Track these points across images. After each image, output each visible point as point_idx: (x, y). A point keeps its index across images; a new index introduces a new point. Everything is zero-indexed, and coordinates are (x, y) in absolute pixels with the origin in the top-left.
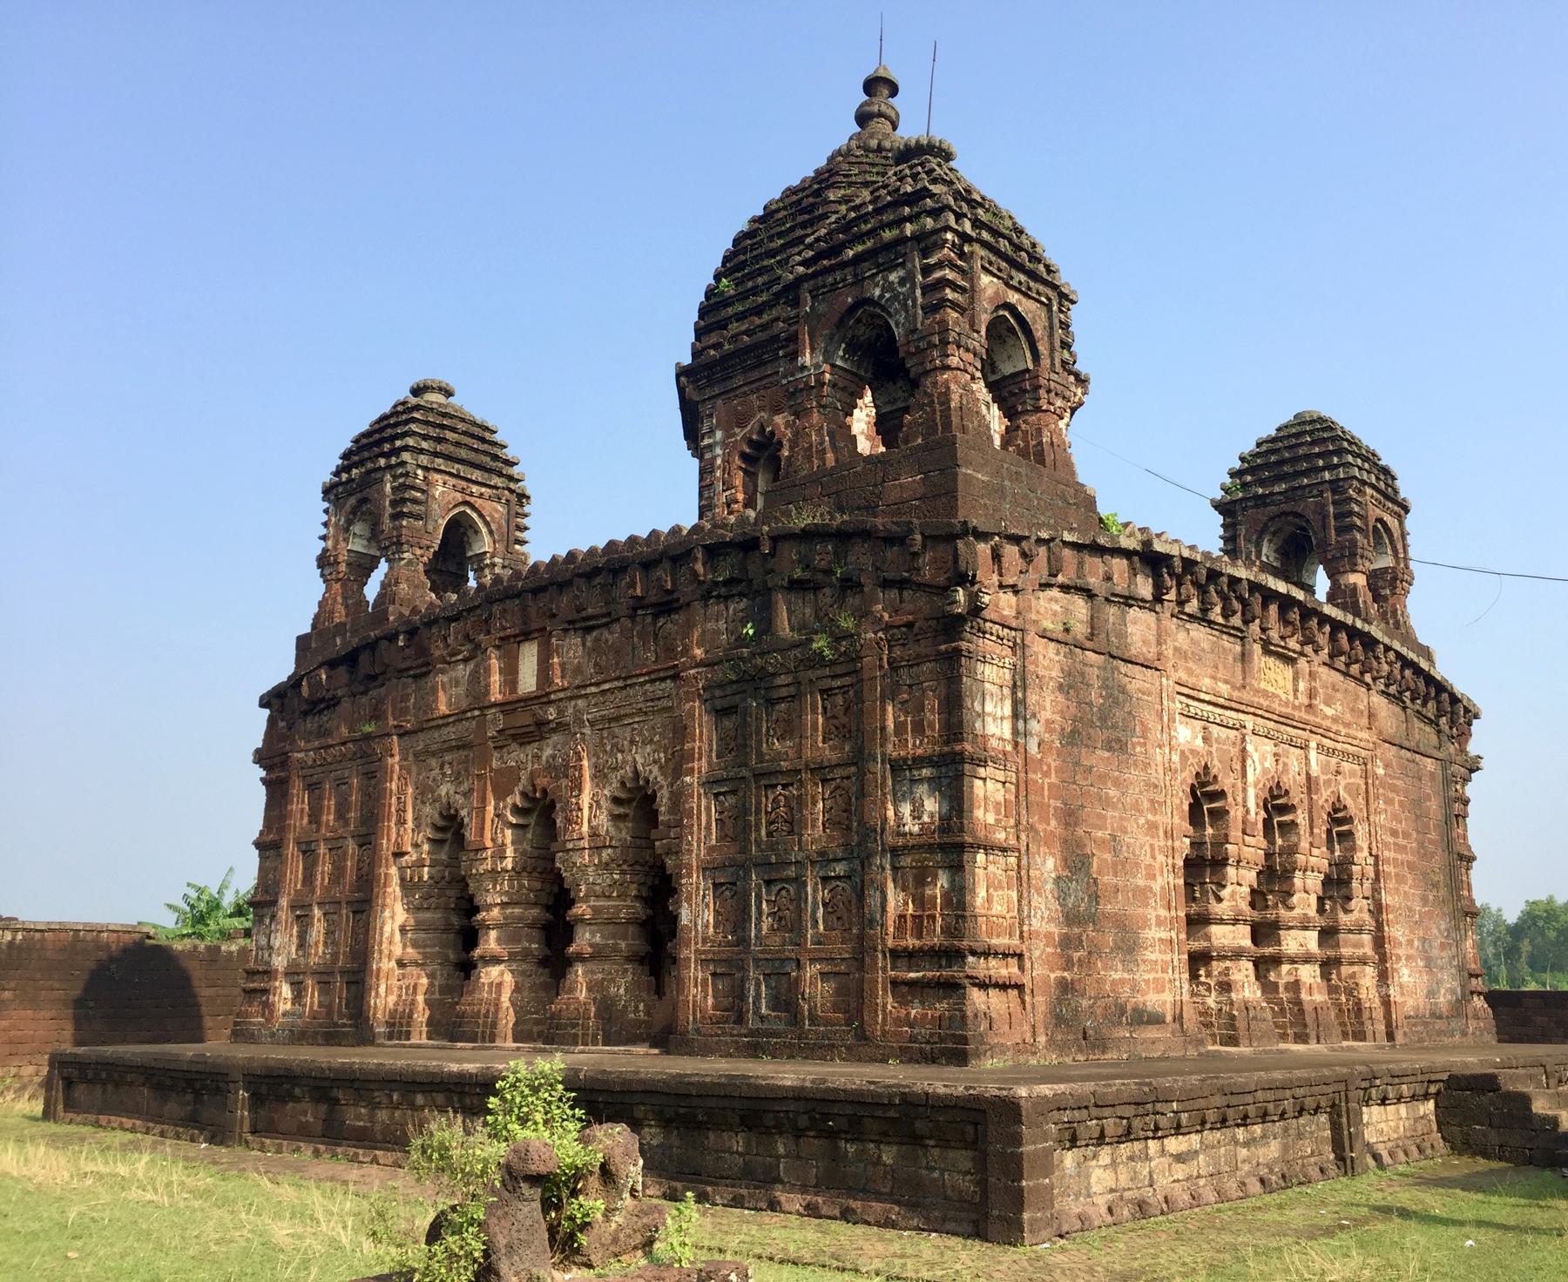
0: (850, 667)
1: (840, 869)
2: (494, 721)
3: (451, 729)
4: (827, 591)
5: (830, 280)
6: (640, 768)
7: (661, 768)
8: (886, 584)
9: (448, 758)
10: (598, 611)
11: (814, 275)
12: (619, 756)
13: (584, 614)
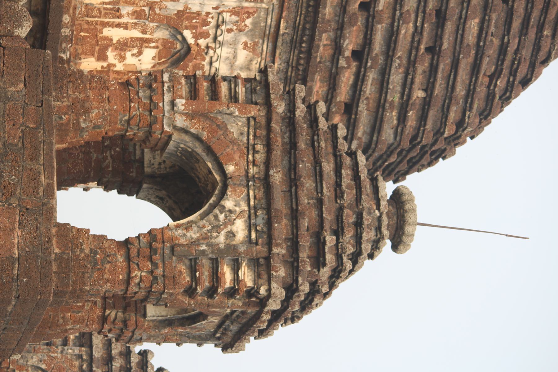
5: (259, 147)
11: (269, 129)
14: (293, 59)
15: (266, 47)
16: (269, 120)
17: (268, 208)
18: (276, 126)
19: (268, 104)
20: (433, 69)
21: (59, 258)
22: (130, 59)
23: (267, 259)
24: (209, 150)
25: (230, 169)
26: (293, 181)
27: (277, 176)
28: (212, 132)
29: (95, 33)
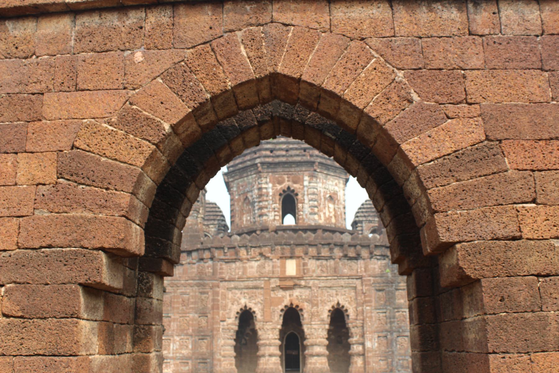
2: (275, 282)
3: (250, 282)
6: (340, 302)
7: (349, 303)
9: (246, 291)
12: (331, 298)
13: (320, 255)
15: (329, 177)
22: (332, 210)
29: (328, 219)
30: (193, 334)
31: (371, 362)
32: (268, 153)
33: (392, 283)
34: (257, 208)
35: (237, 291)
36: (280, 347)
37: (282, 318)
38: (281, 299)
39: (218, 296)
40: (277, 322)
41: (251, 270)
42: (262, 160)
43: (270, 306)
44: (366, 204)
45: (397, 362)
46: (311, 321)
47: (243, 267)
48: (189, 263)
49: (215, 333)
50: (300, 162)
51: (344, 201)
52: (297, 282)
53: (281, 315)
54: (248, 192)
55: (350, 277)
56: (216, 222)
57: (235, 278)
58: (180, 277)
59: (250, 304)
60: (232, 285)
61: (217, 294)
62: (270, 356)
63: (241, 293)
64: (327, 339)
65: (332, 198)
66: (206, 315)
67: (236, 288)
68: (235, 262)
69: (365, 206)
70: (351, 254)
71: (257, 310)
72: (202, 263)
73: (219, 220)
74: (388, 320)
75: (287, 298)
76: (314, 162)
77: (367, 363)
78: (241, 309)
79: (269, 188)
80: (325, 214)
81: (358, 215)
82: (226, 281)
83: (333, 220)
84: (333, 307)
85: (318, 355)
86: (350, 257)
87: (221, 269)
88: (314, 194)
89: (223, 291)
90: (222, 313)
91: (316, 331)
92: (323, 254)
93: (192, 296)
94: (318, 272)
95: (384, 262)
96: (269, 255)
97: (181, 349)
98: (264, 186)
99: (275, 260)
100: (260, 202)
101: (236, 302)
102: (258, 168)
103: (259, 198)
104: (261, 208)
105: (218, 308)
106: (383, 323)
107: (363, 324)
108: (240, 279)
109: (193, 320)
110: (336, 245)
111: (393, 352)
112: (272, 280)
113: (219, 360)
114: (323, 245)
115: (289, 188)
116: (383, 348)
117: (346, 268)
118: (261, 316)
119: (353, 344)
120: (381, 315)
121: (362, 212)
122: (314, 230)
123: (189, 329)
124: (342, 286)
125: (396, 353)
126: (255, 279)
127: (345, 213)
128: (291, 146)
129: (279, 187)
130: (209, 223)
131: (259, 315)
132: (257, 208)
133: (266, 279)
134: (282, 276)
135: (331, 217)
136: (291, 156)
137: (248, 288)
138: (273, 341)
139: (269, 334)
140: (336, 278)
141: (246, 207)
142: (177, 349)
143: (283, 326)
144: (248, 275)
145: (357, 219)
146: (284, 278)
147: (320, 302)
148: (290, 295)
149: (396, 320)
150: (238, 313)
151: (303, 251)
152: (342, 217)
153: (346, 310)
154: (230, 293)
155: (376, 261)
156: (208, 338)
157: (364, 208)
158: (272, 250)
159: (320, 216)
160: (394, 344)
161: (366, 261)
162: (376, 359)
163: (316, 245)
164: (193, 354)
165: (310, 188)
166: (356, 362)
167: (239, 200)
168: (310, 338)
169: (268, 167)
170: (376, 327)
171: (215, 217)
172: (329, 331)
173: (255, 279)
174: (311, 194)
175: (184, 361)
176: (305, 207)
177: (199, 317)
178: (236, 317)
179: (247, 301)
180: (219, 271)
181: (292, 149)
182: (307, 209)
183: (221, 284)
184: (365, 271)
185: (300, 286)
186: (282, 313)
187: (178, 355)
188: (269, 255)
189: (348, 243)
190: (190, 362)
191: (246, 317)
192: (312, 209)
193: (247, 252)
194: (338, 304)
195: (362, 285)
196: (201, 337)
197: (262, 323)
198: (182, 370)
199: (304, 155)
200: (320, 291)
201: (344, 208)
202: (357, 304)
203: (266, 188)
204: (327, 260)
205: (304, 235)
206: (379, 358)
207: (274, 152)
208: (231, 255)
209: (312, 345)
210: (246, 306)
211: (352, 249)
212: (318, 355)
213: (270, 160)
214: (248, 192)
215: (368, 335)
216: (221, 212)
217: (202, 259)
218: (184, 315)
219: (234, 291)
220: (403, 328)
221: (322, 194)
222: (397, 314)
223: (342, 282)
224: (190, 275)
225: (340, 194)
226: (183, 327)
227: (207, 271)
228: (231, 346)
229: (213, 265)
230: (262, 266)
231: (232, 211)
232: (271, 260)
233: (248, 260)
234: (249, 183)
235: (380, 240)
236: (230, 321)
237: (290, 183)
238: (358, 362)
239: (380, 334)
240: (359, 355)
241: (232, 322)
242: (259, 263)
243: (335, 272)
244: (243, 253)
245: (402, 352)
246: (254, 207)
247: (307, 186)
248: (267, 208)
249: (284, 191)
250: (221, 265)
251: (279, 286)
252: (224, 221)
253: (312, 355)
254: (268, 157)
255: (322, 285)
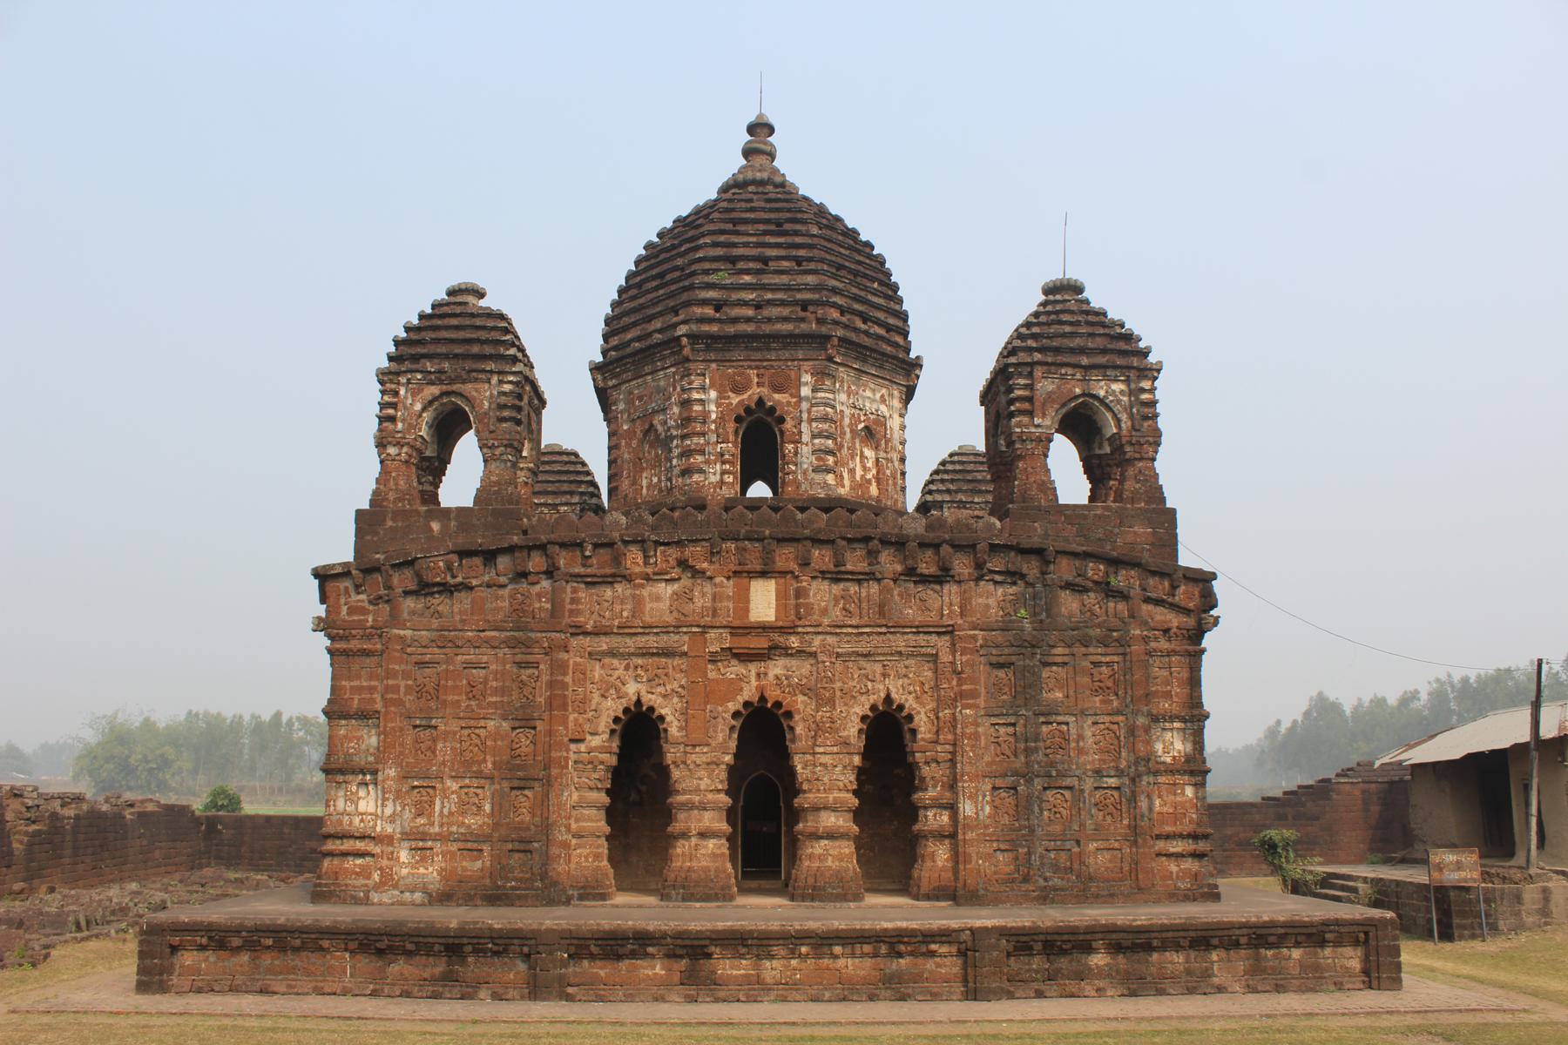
0: (1121, 650)
1: (1112, 782)
2: (720, 639)
4: (1092, 595)
6: (894, 695)
8: (1148, 600)
9: (640, 661)
10: (859, 569)
11: (1052, 364)
12: (870, 685)
14: (871, 361)
16: (1046, 364)
17: (1105, 367)
18: (1050, 360)
19: (1032, 364)
20: (865, 276)
21: (1147, 503)
22: (870, 464)
23: (1139, 369)
24: (1064, 405)
25: (1078, 391)
26: (1082, 351)
27: (1085, 361)
28: (1053, 401)
30: (496, 773)
31: (974, 857)
32: (709, 311)
33: (1033, 646)
34: (676, 452)
35: (615, 662)
36: (731, 815)
37: (735, 736)
38: (736, 685)
39: (565, 674)
40: (722, 744)
41: (655, 605)
42: (694, 327)
43: (706, 703)
44: (953, 463)
45: (1041, 857)
46: (815, 745)
47: (634, 596)
48: (489, 586)
49: (554, 771)
50: (791, 336)
51: (903, 443)
52: (778, 638)
53: (732, 728)
54: (655, 412)
55: (919, 629)
56: (576, 499)
57: (611, 627)
58: (463, 621)
59: (653, 697)
60: (603, 644)
61: (562, 667)
62: (703, 835)
63: (627, 668)
64: (855, 792)
65: (872, 433)
66: (532, 723)
67: (612, 653)
68: (611, 583)
69: (950, 467)
70: (927, 567)
71: (669, 711)
72: (523, 586)
73: (582, 494)
74: (1022, 745)
75: (749, 682)
76: (828, 338)
77: (961, 859)
78: (626, 710)
79: (709, 401)
80: (852, 471)
81: (933, 487)
82: (586, 633)
83: (874, 490)
84: (873, 708)
85: (831, 835)
86: (921, 575)
87: (573, 601)
88: (825, 419)
89: (578, 659)
90: (576, 720)
91: (827, 774)
92: (849, 567)
93: (496, 672)
94: (837, 613)
95: (1012, 590)
96: (705, 565)
97: (463, 813)
98: (696, 396)
99: (718, 580)
100: (684, 437)
101: (613, 691)
102: (682, 347)
103: (682, 426)
104: (687, 453)
105: (564, 707)
106: (1008, 752)
107: (953, 753)
108: (625, 630)
109: (497, 735)
110: (885, 542)
111: (1032, 831)
112: (712, 634)
113: (565, 845)
114: (850, 541)
115: (760, 402)
116: (1006, 820)
117: (911, 605)
118: (680, 728)
119: (926, 808)
120: (1002, 730)
121: (942, 481)
122: (829, 505)
123: (485, 760)
124: (900, 653)
125: (1039, 832)
126: (666, 629)
127: (903, 474)
128: (769, 296)
129: (735, 400)
130: (558, 501)
131: (674, 728)
132: (676, 452)
133: (695, 629)
134: (737, 623)
135: (869, 482)
136: (769, 320)
137: (645, 653)
138: (710, 796)
139: (701, 778)
140: (884, 630)
141: (649, 453)
142: (451, 813)
143: (736, 756)
144: (647, 619)
145: (929, 498)
146: (745, 630)
147: (838, 693)
148: (758, 675)
149: (1041, 744)
150: (616, 720)
151: (797, 558)
152: (895, 484)
153: (910, 718)
154: (598, 666)
155: (991, 587)
156: (536, 784)
157: (946, 472)
158: (713, 554)
159: (842, 477)
160: (1036, 809)
161: (964, 586)
162: (987, 848)
163: (832, 542)
164: (496, 827)
165: (817, 405)
166: (933, 854)
167: (631, 434)
168: (810, 791)
169: (708, 348)
170: (989, 764)
171: (573, 487)
172: (861, 772)
173: (666, 629)
174: (816, 420)
175: (469, 845)
176: (802, 456)
177: (514, 729)
178: (613, 732)
179: (643, 689)
180: (568, 607)
181: (770, 302)
182: (807, 458)
183: (574, 642)
184: (962, 614)
185: (786, 652)
186: (737, 723)
187: (454, 829)
188: (705, 565)
189: (916, 536)
190: (486, 848)
191: (639, 731)
192: (819, 459)
193: (646, 557)
194: (888, 699)
195: (953, 652)
196: (516, 783)
197: (682, 748)
198: (465, 869)
199: (803, 320)
200: (839, 666)
201: (903, 460)
202: (938, 700)
203: (702, 402)
204: (859, 581)
205: (799, 516)
206: (995, 845)
207: (725, 309)
208: (601, 566)
209: (816, 809)
210: (639, 703)
211: (929, 553)
212: (831, 835)
213: (714, 328)
214: (655, 412)
215: (965, 785)
216: (588, 473)
217: (524, 575)
218: (473, 723)
219: (607, 660)
220: (1060, 767)
221: (847, 421)
222: (1044, 729)
223: (899, 642)
224: (490, 617)
225: (895, 423)
226: (468, 756)
227: (537, 605)
228: (599, 808)
229: (554, 590)
230: (685, 596)
231: (612, 463)
232: (711, 578)
233: (647, 578)
234: (659, 390)
235: (1001, 530)
236: (595, 741)
237: (765, 391)
238: (941, 854)
239: (999, 782)
240: (940, 836)
241: (600, 743)
242: (676, 586)
243: (882, 613)
244: (634, 559)
245: (1057, 828)
246: (670, 451)
247: (807, 399)
248: (702, 452)
249: (748, 410)
250: (575, 591)
251: (730, 649)
252: (599, 496)
253: (816, 836)
254: (710, 321)
255: (846, 648)
